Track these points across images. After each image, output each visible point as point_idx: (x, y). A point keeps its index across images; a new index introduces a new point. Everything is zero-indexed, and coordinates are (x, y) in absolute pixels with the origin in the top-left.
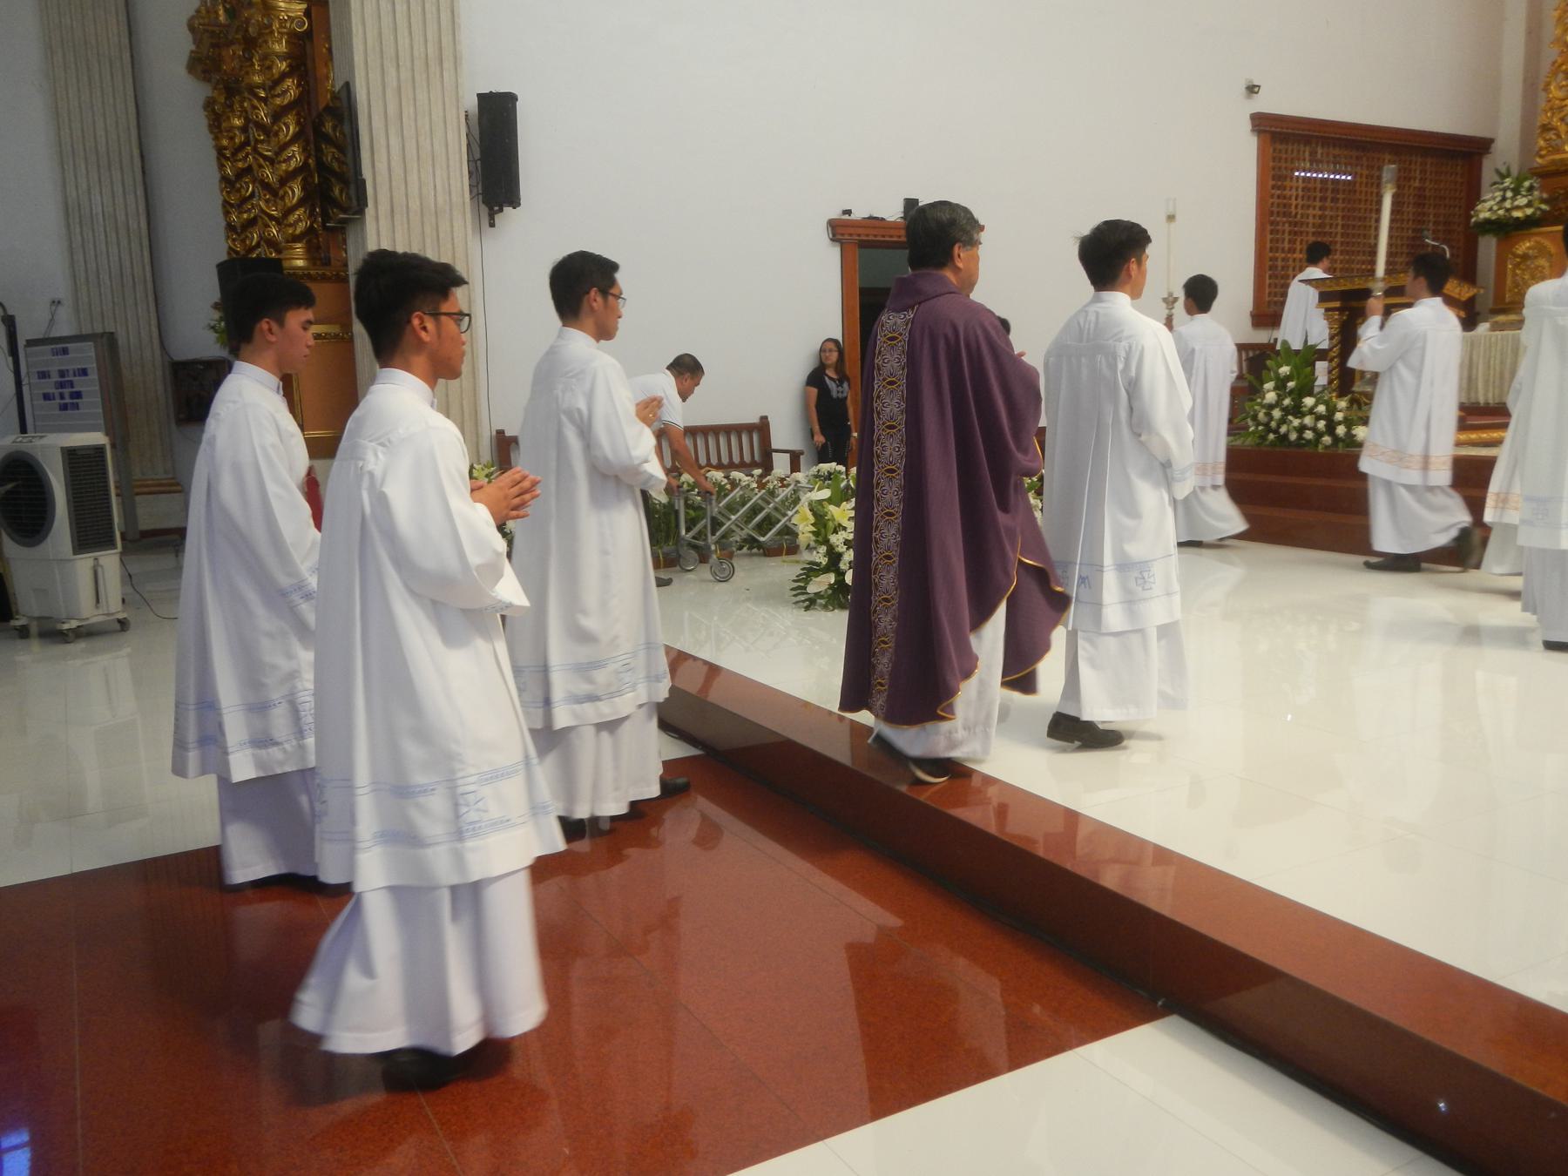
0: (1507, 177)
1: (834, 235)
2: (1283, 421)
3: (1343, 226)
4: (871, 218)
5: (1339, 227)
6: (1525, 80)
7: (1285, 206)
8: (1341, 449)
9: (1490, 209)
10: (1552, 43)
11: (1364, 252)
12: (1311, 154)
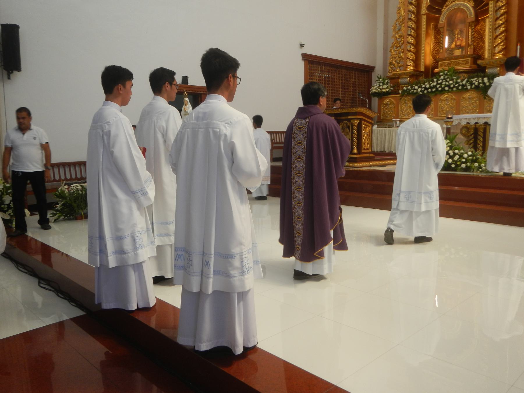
0: (381, 79)
3: (331, 93)
5: (330, 93)
6: (384, 49)
9: (376, 89)
10: (392, 37)
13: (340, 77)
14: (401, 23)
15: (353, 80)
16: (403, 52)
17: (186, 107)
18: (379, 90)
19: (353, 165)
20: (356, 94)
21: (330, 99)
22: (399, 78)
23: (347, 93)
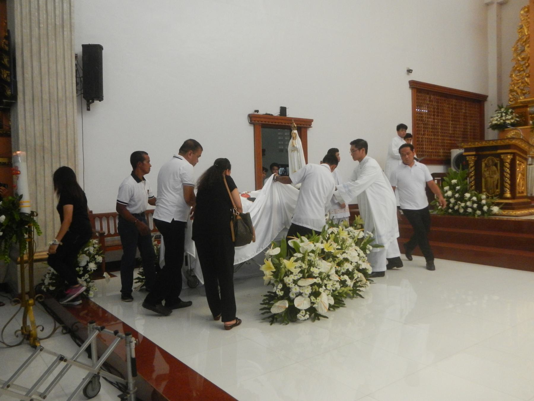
1: (251, 121)
2: (455, 204)
3: (441, 126)
4: (266, 114)
7: (421, 117)
8: (486, 217)
9: (497, 120)
10: (513, 60)
11: (448, 136)
12: (429, 98)
14: (524, 44)
15: (464, 111)
16: (527, 77)
17: (294, 141)
19: (509, 213)
21: (440, 133)
22: (527, 106)
23: (458, 126)
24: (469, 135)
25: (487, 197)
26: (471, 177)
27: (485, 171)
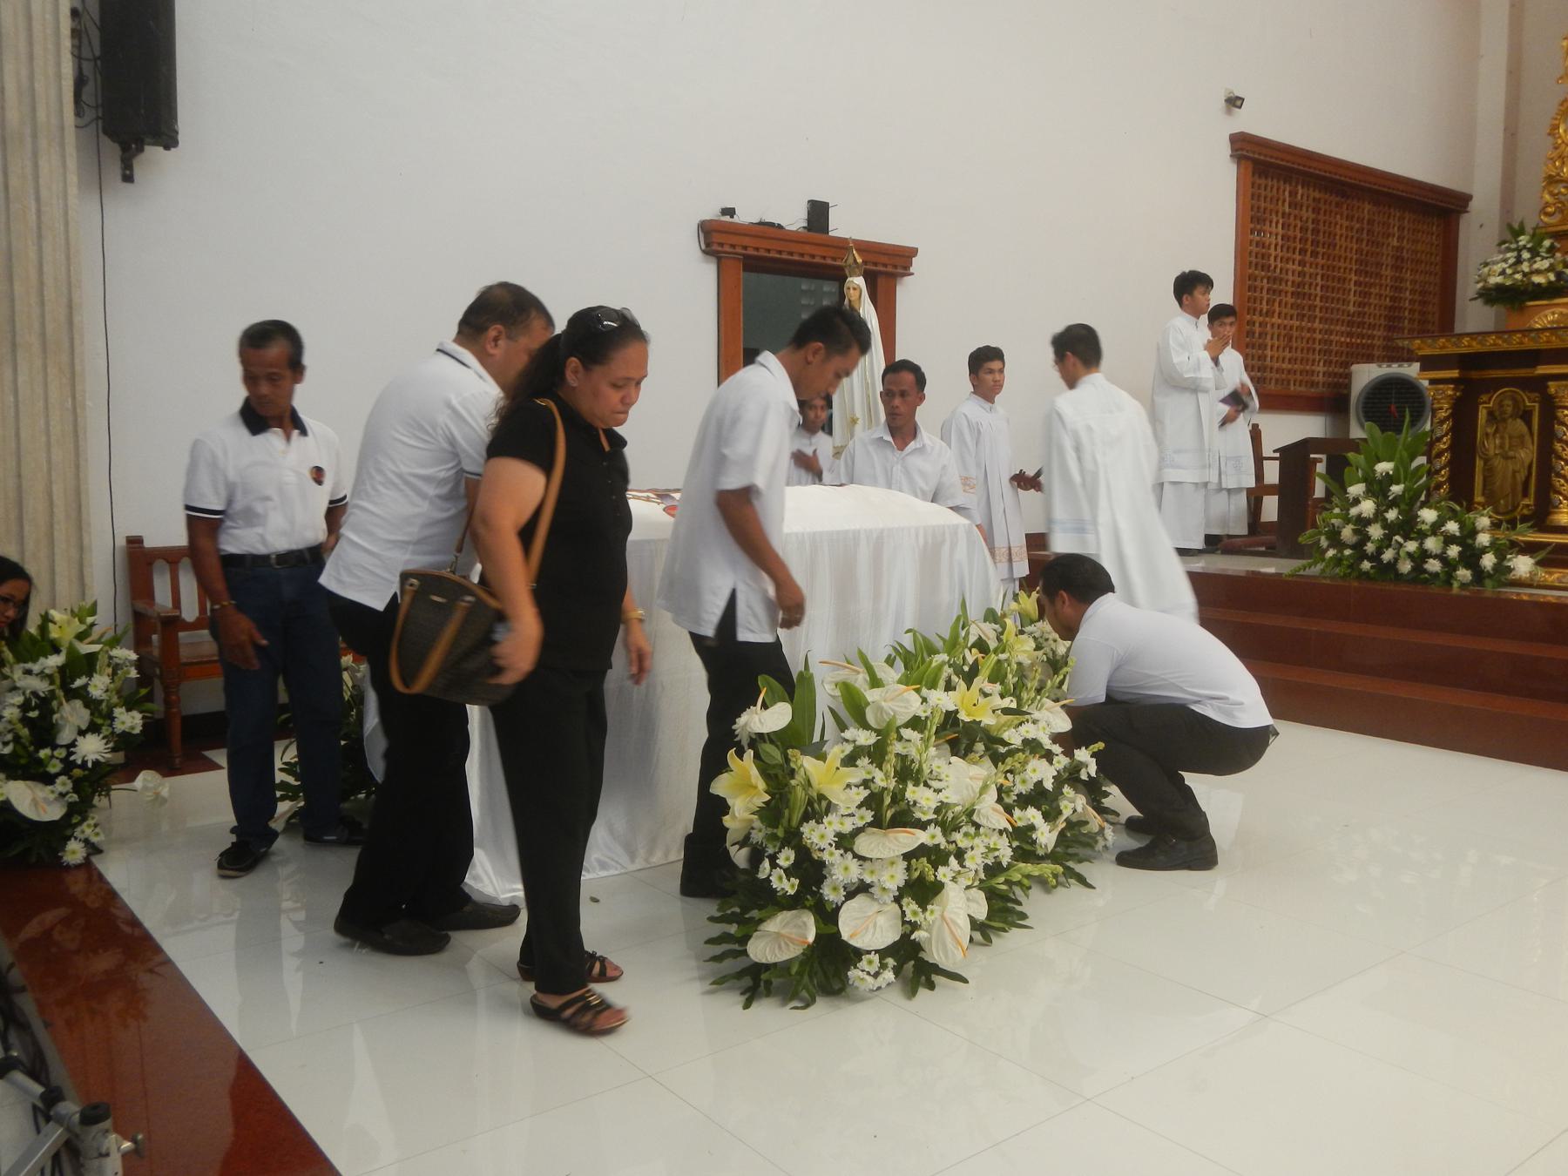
0: (1523, 234)
1: (708, 245)
2: (1386, 542)
4: (761, 223)
8: (1489, 588)
9: (1503, 273)
12: (1290, 193)
13: (1352, 229)
15: (1395, 243)
18: (1518, 276)
20: (1402, 295)
24: (1406, 321)
25: (1496, 525)
26: (1439, 455)
27: (1487, 435)
